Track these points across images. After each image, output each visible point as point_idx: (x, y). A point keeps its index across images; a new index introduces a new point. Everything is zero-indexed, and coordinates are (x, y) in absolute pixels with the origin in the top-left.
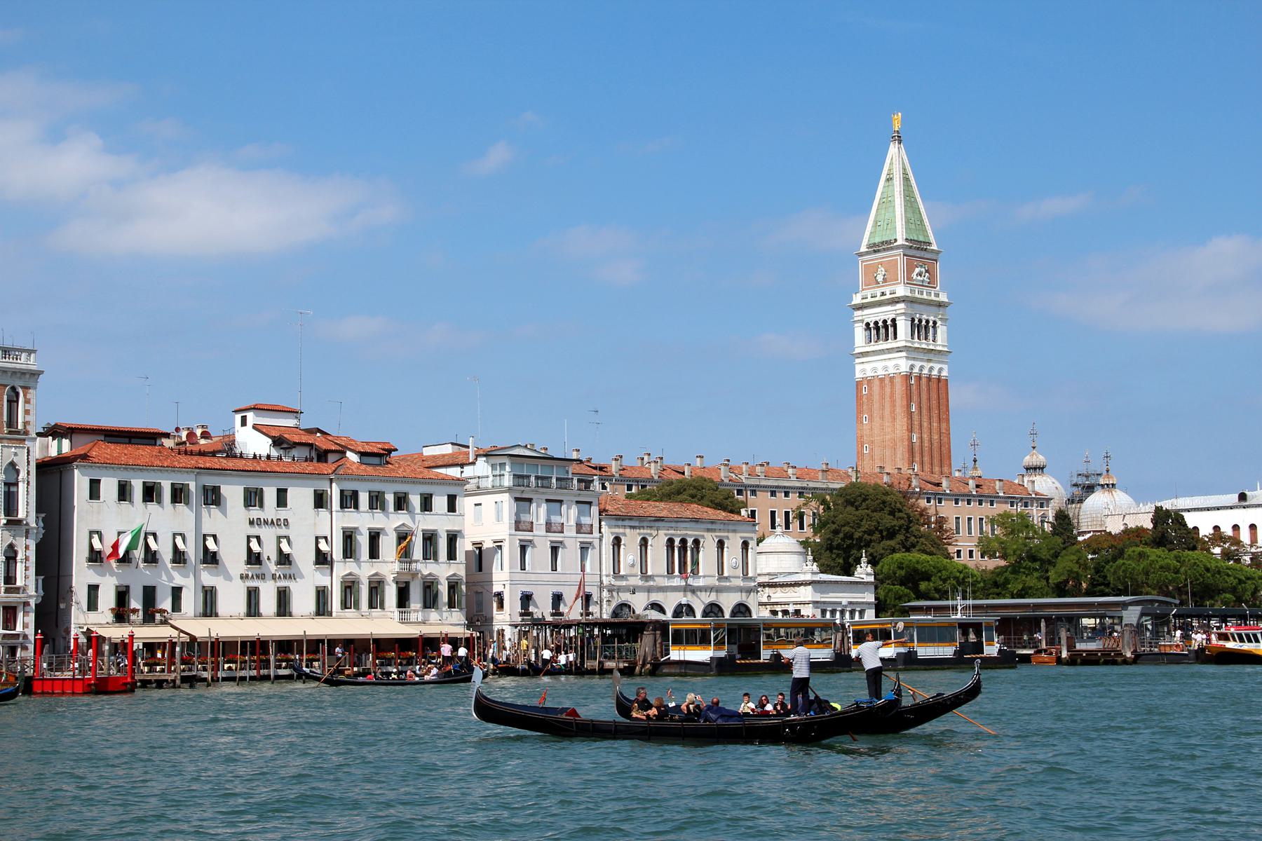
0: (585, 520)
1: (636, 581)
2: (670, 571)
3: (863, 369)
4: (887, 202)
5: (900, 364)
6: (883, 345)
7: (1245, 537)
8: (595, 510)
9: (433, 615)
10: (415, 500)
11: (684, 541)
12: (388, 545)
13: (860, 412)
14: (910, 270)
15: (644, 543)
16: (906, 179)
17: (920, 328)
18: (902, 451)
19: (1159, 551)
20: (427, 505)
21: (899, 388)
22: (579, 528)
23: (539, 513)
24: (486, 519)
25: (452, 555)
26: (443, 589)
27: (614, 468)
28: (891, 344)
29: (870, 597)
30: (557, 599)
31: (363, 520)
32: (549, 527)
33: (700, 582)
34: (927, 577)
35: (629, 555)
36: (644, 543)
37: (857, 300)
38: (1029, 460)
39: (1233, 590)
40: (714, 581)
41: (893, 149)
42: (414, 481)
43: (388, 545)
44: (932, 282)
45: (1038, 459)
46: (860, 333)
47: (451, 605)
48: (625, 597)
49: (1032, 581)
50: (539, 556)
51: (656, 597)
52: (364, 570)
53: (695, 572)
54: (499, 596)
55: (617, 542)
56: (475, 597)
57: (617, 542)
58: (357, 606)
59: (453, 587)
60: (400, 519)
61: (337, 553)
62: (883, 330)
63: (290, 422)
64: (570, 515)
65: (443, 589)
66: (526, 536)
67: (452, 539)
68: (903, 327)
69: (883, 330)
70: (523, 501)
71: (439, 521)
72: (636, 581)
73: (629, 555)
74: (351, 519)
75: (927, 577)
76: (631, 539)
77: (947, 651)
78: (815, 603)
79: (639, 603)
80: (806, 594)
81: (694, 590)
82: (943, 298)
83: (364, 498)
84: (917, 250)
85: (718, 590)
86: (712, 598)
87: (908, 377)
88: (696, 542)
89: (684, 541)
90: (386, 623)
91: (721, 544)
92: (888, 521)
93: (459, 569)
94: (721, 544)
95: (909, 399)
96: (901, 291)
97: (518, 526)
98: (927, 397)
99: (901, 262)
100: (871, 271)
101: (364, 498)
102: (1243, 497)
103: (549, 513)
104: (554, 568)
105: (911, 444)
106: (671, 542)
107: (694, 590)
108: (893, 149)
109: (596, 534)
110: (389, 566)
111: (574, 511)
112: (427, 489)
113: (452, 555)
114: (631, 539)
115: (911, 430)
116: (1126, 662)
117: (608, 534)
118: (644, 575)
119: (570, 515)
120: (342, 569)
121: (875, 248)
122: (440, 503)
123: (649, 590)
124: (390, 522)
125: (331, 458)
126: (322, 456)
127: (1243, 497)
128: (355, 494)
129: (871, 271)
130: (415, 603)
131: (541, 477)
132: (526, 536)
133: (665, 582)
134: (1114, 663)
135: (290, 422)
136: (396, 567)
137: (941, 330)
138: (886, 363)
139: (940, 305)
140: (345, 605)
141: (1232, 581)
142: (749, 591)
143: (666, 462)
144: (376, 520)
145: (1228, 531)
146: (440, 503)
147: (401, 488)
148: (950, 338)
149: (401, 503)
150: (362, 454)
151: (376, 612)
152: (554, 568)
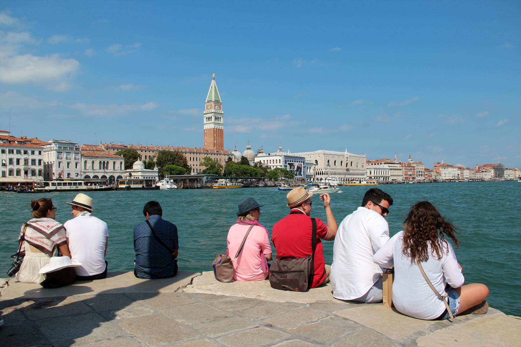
0: (77, 157)
1: (91, 170)
2: (100, 168)
3: (206, 127)
4: (211, 92)
5: (212, 126)
6: (209, 122)
7: (266, 162)
8: (80, 155)
9: (34, 178)
10: (30, 152)
11: (104, 162)
12: (22, 162)
13: (205, 136)
14: (215, 106)
15: (93, 162)
16: (215, 88)
17: (216, 118)
18: (212, 144)
19: (243, 166)
20: (33, 153)
21: (212, 131)
22: (75, 159)
23: (64, 155)
24: (50, 157)
25: (40, 164)
26: (37, 172)
27: (110, 145)
28: (211, 122)
29: (157, 175)
30: (69, 174)
31: (15, 156)
32: (67, 158)
33: (109, 171)
34: (173, 170)
35: (89, 165)
36: (93, 162)
37: (204, 112)
38: (248, 147)
39: (250, 173)
40: (112, 171)
41: (213, 81)
42: (29, 148)
43: (22, 162)
44: (220, 109)
45: (250, 147)
46: (205, 119)
47: (40, 175)
48: (87, 174)
49: (210, 171)
50: (72, 165)
51: (96, 174)
52: (15, 167)
53: (107, 169)
54: (54, 173)
55: (86, 162)
56: (47, 173)
57: (86, 162)
58: (13, 175)
59: (40, 171)
60: (26, 156)
61: (8, 163)
62: (209, 119)
63: (7, 135)
64: (73, 156)
65: (37, 172)
66: (61, 160)
67: (40, 161)
68: (213, 118)
69: (209, 119)
70: (59, 152)
71: (36, 157)
72: (91, 170)
73: (89, 165)
74: (11, 156)
75: (173, 170)
76: (89, 162)
77: (141, 186)
78: (142, 176)
79: (91, 175)
80: (140, 174)
81: (107, 173)
82: (222, 112)
83: (15, 151)
84: (217, 102)
85: (113, 173)
86: (112, 174)
87: (214, 129)
88: (108, 162)
89: (104, 162)
90: (21, 179)
91: (114, 163)
92: (169, 158)
93: (42, 167)
94: (114, 163)
95: (214, 133)
96: (213, 111)
97: (58, 158)
98: (218, 133)
99: (213, 104)
100: (207, 106)
101: (15, 151)
102: (269, 154)
103: (67, 155)
104: (76, 167)
105: (214, 143)
106: (100, 162)
107: (107, 173)
108: (213, 81)
109: (80, 160)
110: (22, 166)
111: (74, 155)
112: (33, 150)
113: (40, 164)
114: (89, 162)
115: (214, 140)
116: (195, 188)
117: (83, 160)
118: (93, 168)
119: (73, 156)
120: (9, 167)
121: (208, 102)
122: (37, 152)
123: (94, 172)
124: (22, 157)
125: (12, 142)
126: (10, 142)
127: (269, 154)
128: (13, 151)
129: (207, 106)
130: (30, 174)
131: (65, 147)
132: (77, 161)
133: (99, 171)
134: (192, 188)
135: (7, 135)
136: (23, 167)
137: (222, 119)
138: (209, 126)
139: (222, 114)
140: (10, 175)
141: (249, 171)
142: (122, 173)
143: (142, 146)
144: (19, 156)
145: (262, 162)
146: (37, 152)
147: (26, 149)
148: (224, 120)
149: (26, 153)
150: (18, 142)
151: (18, 177)
152: (76, 167)
